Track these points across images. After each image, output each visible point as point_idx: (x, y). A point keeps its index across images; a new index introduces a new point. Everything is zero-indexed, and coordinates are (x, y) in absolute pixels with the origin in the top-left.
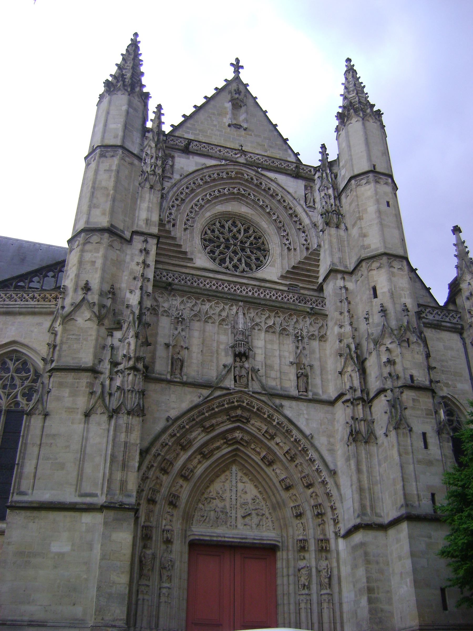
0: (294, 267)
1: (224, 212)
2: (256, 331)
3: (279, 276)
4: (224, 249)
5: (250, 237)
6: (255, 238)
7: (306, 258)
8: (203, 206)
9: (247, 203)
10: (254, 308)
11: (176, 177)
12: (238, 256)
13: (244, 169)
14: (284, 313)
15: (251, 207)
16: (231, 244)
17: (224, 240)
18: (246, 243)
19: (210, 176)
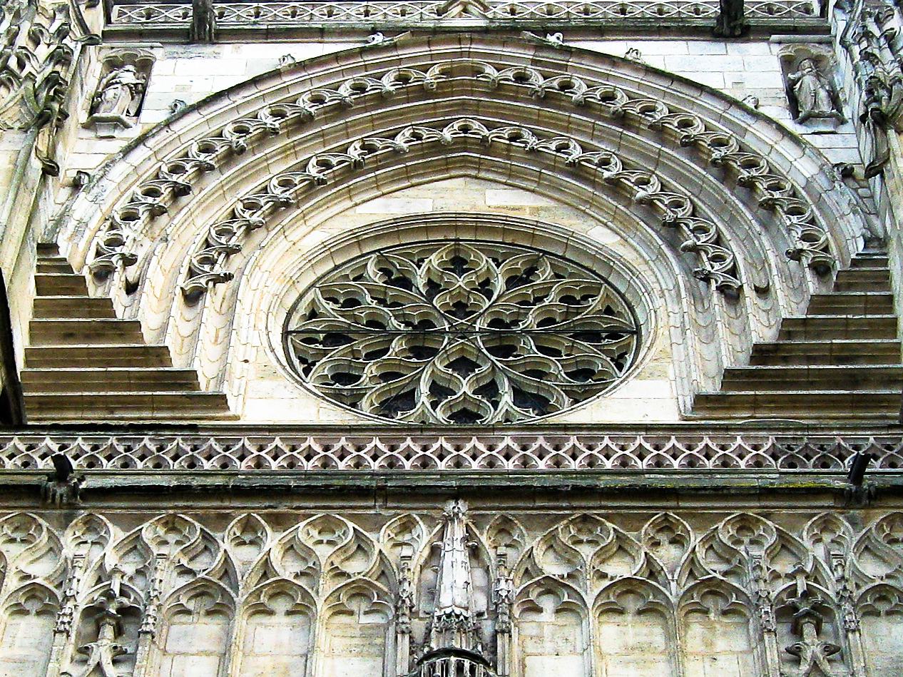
0: (761, 353)
2: (548, 616)
3: (689, 404)
6: (567, 299)
7: (817, 304)
9: (510, 173)
10: (530, 523)
11: (154, 114)
13: (481, 48)
14: (701, 520)
15: (533, 186)
18: (515, 323)
19: (318, 100)
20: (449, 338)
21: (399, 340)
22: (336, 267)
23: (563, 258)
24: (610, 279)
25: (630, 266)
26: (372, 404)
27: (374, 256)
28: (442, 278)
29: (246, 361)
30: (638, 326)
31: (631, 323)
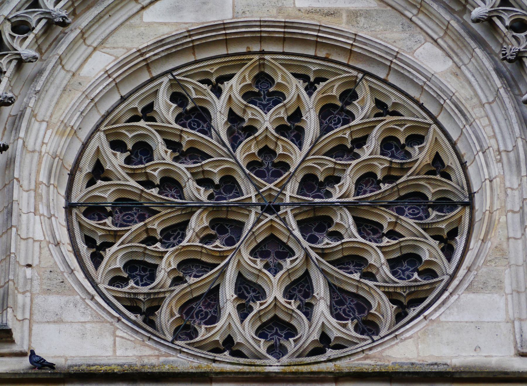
1: (190, 33)
4: (208, 239)
5: (360, 142)
8: (64, 24)
12: (287, 264)
16: (246, 205)
17: (203, 195)
20: (256, 213)
21: (200, 214)
22: (123, 99)
23: (385, 81)
24: (440, 119)
25: (463, 108)
26: (172, 315)
27: (165, 80)
28: (245, 111)
29: (29, 266)
30: (471, 195)
31: (463, 188)
